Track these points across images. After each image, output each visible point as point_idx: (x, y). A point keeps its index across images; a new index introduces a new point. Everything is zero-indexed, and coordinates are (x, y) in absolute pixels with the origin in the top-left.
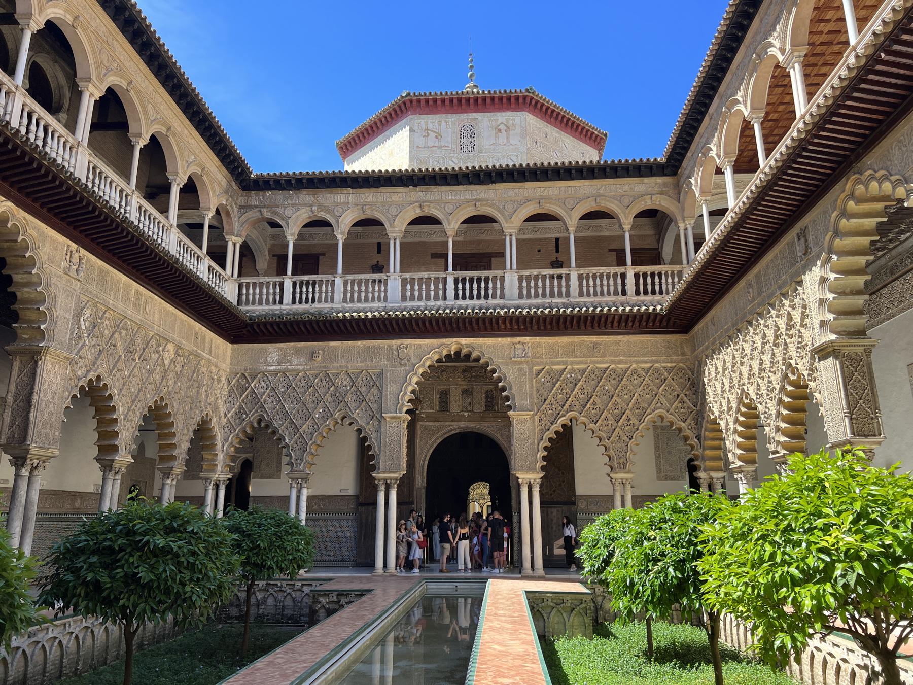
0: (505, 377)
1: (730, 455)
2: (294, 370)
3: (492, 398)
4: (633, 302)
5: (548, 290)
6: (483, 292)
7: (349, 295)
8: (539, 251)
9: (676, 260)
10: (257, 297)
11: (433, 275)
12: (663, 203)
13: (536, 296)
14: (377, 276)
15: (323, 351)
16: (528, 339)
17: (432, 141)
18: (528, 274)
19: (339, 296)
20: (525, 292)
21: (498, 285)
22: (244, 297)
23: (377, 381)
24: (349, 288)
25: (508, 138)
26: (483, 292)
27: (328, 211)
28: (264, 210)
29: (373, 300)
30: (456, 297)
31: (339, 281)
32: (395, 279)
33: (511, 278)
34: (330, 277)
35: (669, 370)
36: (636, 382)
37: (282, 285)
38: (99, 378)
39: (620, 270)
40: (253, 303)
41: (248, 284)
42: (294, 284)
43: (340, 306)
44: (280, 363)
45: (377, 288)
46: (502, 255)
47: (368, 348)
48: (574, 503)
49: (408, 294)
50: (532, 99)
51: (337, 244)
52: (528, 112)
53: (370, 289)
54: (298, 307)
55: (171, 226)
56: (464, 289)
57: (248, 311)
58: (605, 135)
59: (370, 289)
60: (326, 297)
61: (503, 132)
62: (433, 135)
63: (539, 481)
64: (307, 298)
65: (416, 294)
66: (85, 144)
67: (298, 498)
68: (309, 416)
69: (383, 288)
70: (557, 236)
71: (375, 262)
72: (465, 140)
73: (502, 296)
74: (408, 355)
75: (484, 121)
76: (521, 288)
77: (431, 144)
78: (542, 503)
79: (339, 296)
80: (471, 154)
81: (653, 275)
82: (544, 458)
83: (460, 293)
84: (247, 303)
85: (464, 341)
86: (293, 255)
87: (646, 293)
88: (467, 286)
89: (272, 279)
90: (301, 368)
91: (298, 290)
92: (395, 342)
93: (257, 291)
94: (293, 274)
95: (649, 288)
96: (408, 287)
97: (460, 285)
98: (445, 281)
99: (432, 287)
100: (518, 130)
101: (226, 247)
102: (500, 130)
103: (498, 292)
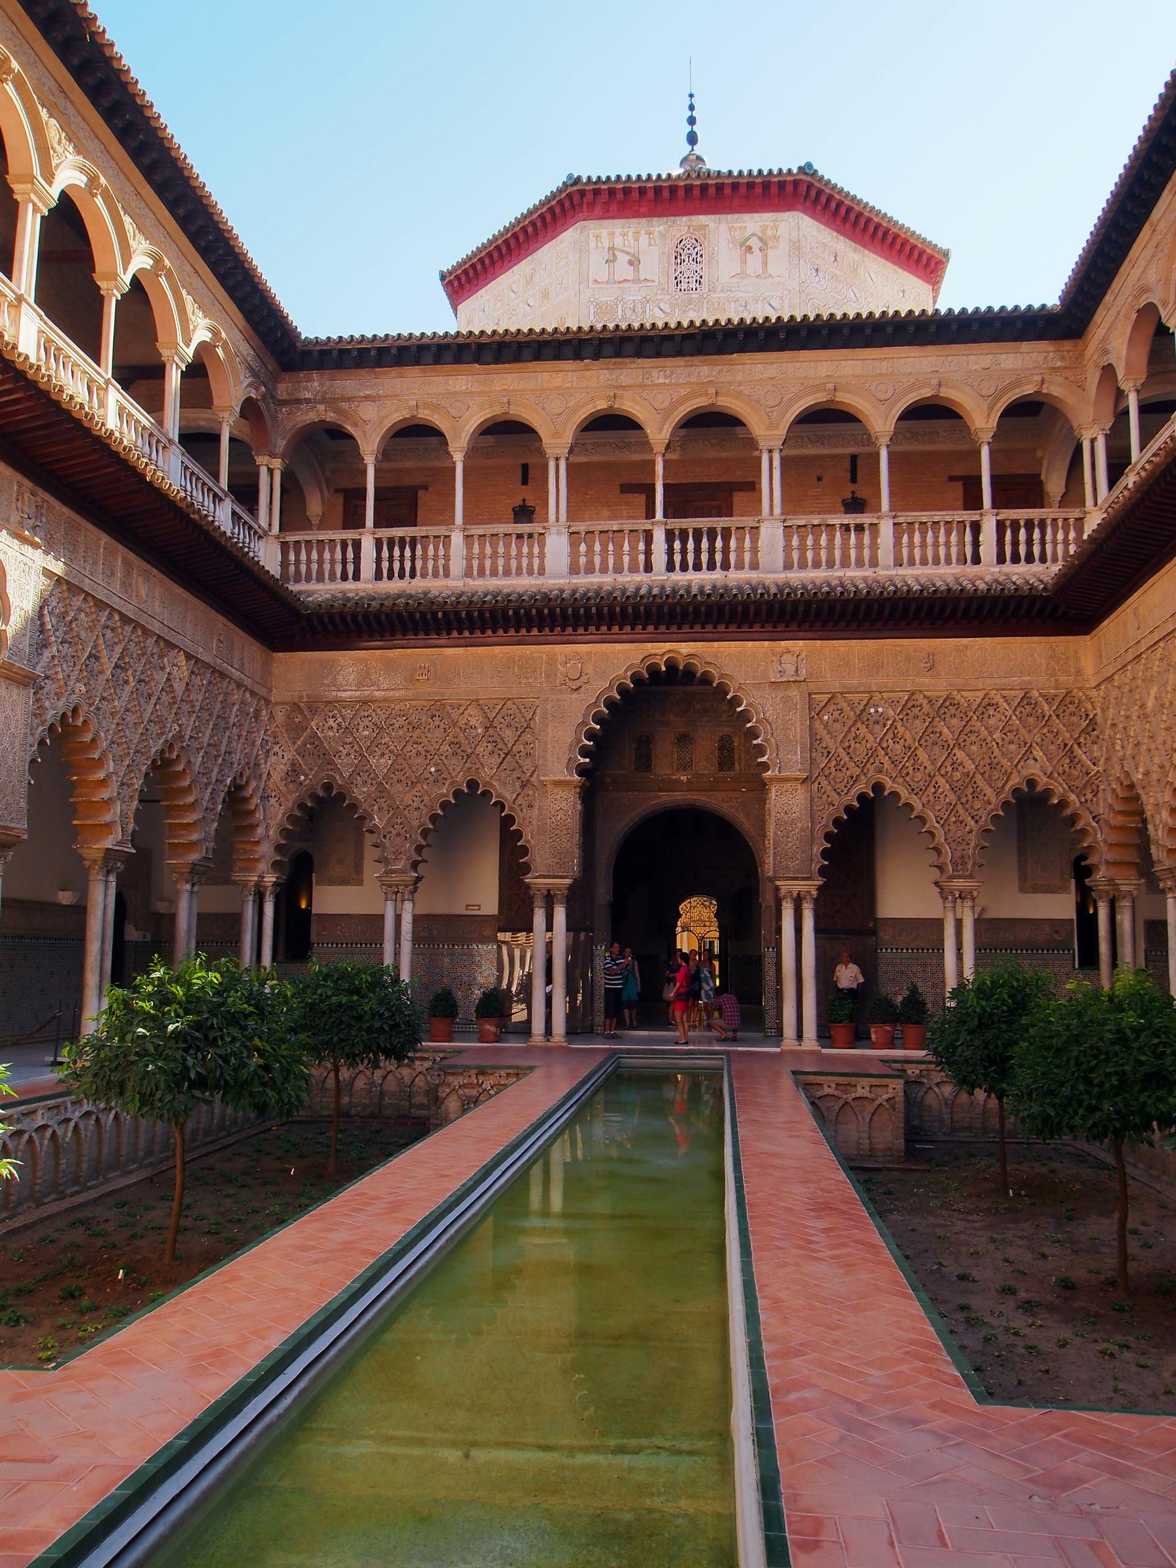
0: (758, 713)
2: (385, 700)
3: (731, 750)
4: (989, 573)
5: (838, 554)
6: (718, 557)
7: (475, 563)
8: (819, 479)
9: (1073, 494)
10: (315, 567)
11: (628, 525)
12: (1056, 389)
13: (817, 565)
14: (524, 528)
17: (623, 269)
19: (457, 565)
20: (795, 555)
22: (292, 568)
24: (476, 549)
25: (765, 264)
26: (718, 557)
27: (436, 408)
28: (321, 407)
29: (519, 572)
30: (670, 567)
31: (457, 539)
32: (559, 533)
33: (771, 534)
34: (441, 530)
35: (1049, 700)
36: (992, 722)
37: (357, 545)
38: (75, 711)
39: (969, 516)
40: (308, 579)
41: (297, 543)
42: (379, 544)
43: (461, 583)
44: (360, 685)
45: (525, 550)
46: (752, 487)
48: (873, 932)
49: (583, 560)
50: (810, 186)
51: (454, 469)
52: (805, 211)
53: (514, 552)
55: (170, 441)
56: (684, 551)
57: (300, 592)
58: (946, 254)
59: (514, 552)
60: (435, 567)
61: (756, 250)
62: (623, 259)
63: (815, 893)
64: (402, 569)
65: (597, 560)
66: (32, 300)
67: (398, 919)
69: (536, 550)
70: (853, 450)
71: (518, 502)
72: (683, 268)
73: (755, 566)
75: (722, 231)
76: (788, 548)
77: (618, 277)
78: (818, 930)
79: (457, 565)
80: (695, 295)
81: (1029, 525)
82: (825, 854)
83: (677, 558)
84: (297, 580)
85: (685, 648)
87: (1016, 559)
88: (691, 545)
89: (339, 535)
90: (397, 694)
91: (385, 553)
92: (561, 651)
93: (315, 556)
94: (377, 525)
95: (1022, 550)
96: (583, 548)
97: (677, 545)
98: (649, 537)
99: (626, 547)
100: (784, 246)
101: (257, 475)
102: (750, 248)
103: (747, 557)
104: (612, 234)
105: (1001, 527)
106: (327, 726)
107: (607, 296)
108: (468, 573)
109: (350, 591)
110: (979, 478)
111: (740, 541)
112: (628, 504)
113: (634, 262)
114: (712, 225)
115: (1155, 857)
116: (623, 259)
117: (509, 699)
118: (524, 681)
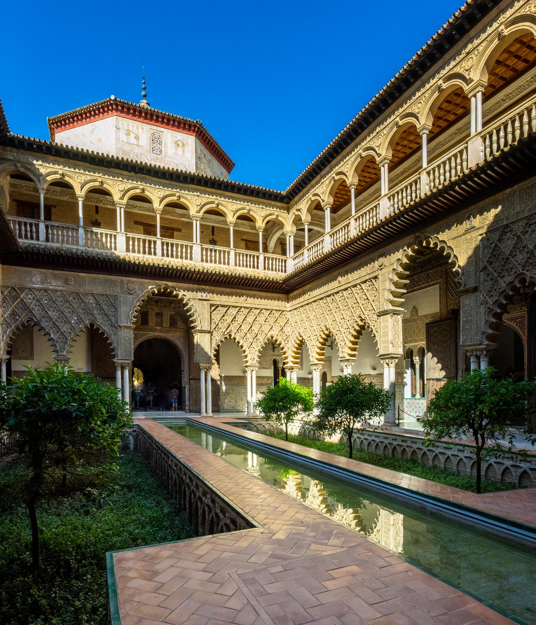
1: (311, 357)
4: (261, 273)
15: (75, 278)
16: (208, 287)
17: (132, 140)
18: (207, 247)
19: (82, 241)
20: (204, 257)
21: (189, 251)
23: (113, 302)
25: (184, 152)
33: (197, 249)
39: (255, 253)
42: (47, 227)
43: (84, 248)
47: (107, 280)
54: (50, 244)
61: (181, 146)
62: (132, 136)
68: (68, 322)
73: (191, 259)
74: (134, 289)
75: (170, 136)
80: (159, 157)
85: (170, 284)
86: (44, 205)
102: (178, 145)
104: (128, 125)
105: (265, 258)
106: (28, 298)
107: (127, 148)
108: (86, 245)
109: (35, 244)
110: (258, 242)
111: (177, 248)
112: (136, 228)
113: (137, 138)
114: (165, 132)
115: (311, 360)
116: (132, 136)
117: (106, 295)
118: (111, 289)
